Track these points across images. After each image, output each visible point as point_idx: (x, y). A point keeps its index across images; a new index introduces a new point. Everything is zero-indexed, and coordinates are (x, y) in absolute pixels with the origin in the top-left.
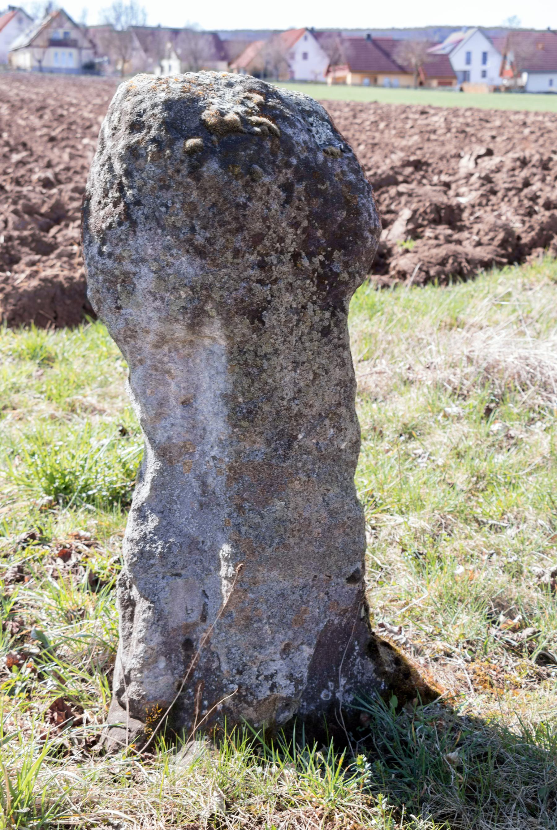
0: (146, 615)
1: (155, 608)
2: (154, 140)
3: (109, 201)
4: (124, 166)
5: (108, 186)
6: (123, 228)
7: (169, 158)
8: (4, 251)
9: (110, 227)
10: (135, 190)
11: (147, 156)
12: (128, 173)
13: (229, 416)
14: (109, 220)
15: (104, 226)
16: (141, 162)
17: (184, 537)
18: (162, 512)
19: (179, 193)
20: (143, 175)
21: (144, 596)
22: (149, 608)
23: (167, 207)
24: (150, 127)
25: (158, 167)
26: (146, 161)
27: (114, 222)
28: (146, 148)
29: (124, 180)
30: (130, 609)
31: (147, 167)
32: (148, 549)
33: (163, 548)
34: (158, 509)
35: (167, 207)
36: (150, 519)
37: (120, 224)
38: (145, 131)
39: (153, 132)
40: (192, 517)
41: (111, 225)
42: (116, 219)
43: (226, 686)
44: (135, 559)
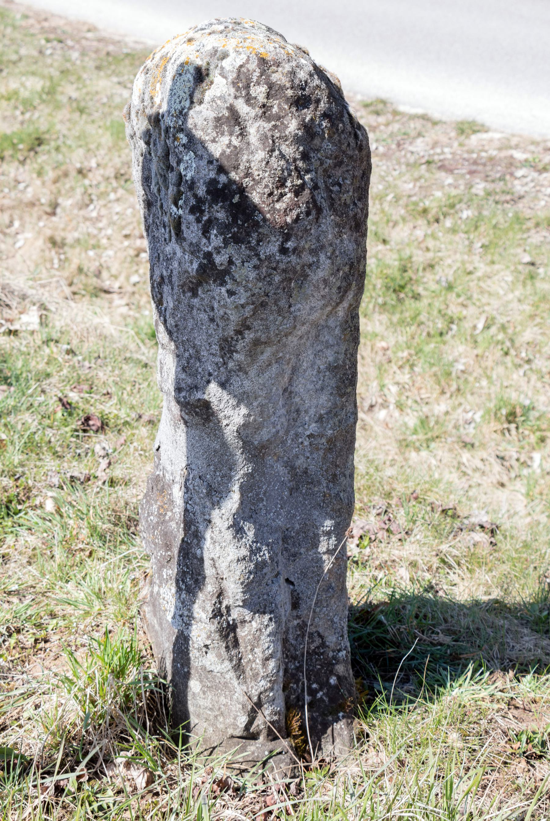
0: (270, 629)
1: (275, 617)
2: (325, 115)
3: (287, 190)
4: (301, 148)
5: (286, 174)
6: (311, 217)
7: (343, 132)
8: (515, 274)
9: (297, 220)
10: (314, 173)
11: (324, 132)
12: (305, 156)
13: (338, 387)
14: (294, 213)
15: (289, 220)
16: (317, 141)
17: (276, 531)
18: (251, 517)
19: (350, 168)
20: (319, 155)
21: (258, 611)
22: (271, 619)
23: (340, 185)
24: (318, 101)
25: (334, 144)
26: (323, 138)
27: (301, 213)
28: (320, 125)
29: (300, 164)
30: (232, 635)
31: (324, 145)
32: (260, 559)
33: (269, 553)
34: (246, 515)
35: (340, 185)
36: (246, 528)
37: (308, 214)
38: (312, 107)
39: (323, 105)
40: (282, 508)
41: (298, 216)
42: (303, 208)
43: (334, 658)
44: (252, 577)
